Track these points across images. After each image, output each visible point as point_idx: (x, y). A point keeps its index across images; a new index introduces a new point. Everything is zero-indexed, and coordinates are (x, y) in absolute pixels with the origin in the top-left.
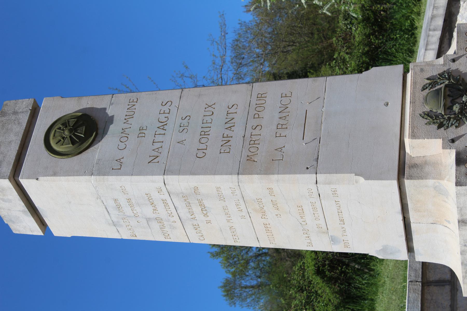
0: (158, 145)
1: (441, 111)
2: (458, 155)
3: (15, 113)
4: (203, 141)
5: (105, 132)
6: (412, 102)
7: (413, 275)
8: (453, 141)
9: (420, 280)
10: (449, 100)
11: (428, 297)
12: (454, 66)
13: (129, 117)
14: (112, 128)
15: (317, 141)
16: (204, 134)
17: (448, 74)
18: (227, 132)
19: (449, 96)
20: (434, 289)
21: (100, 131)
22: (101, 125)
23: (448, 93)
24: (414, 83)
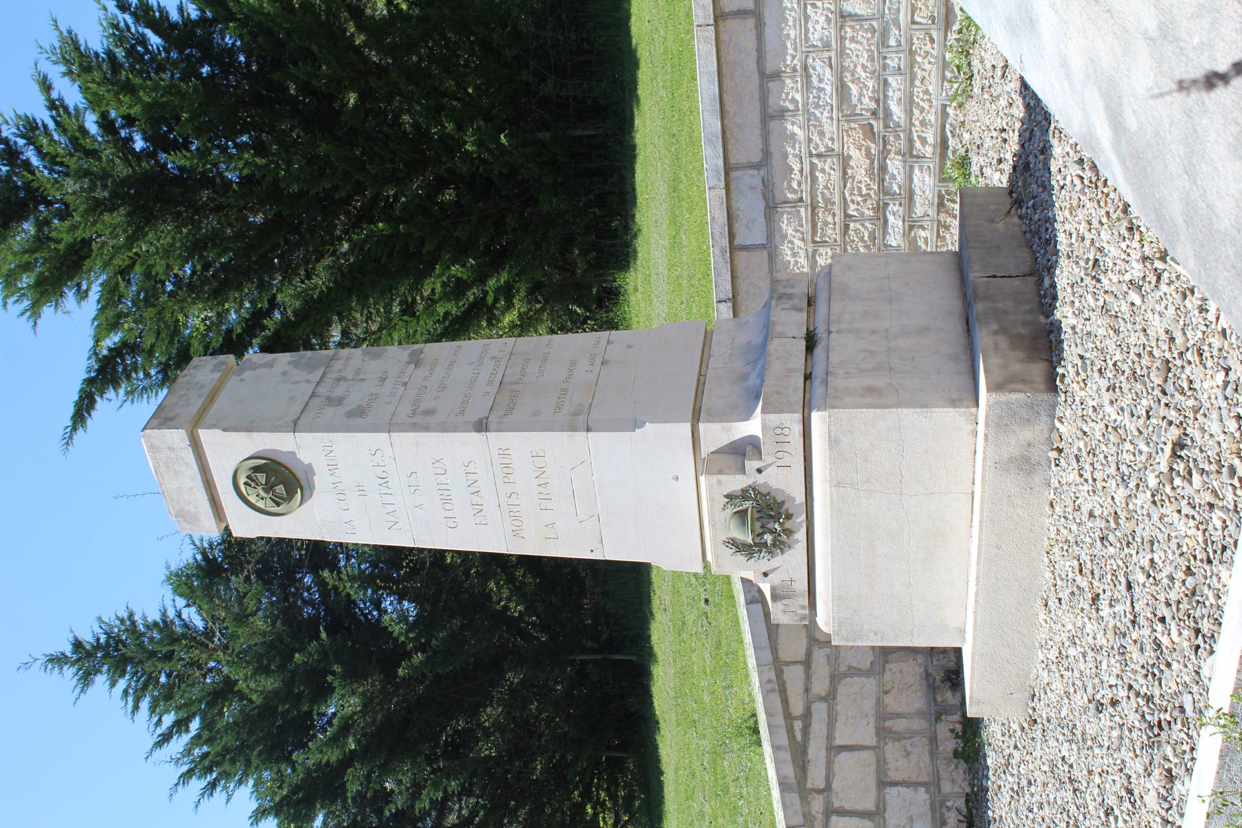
0: (391, 508)
1: (750, 541)
2: (773, 589)
3: (170, 449)
4: (448, 507)
5: (312, 488)
6: (713, 525)
7: (701, 15)
8: (765, 574)
9: (712, 22)
10: (758, 524)
11: (724, 37)
12: (761, 479)
13: (333, 468)
14: (318, 481)
15: (595, 519)
16: (447, 500)
17: (754, 489)
18: (475, 499)
19: (758, 519)
20: (732, 24)
21: (304, 483)
22: (300, 475)
23: (757, 515)
24: (711, 500)
